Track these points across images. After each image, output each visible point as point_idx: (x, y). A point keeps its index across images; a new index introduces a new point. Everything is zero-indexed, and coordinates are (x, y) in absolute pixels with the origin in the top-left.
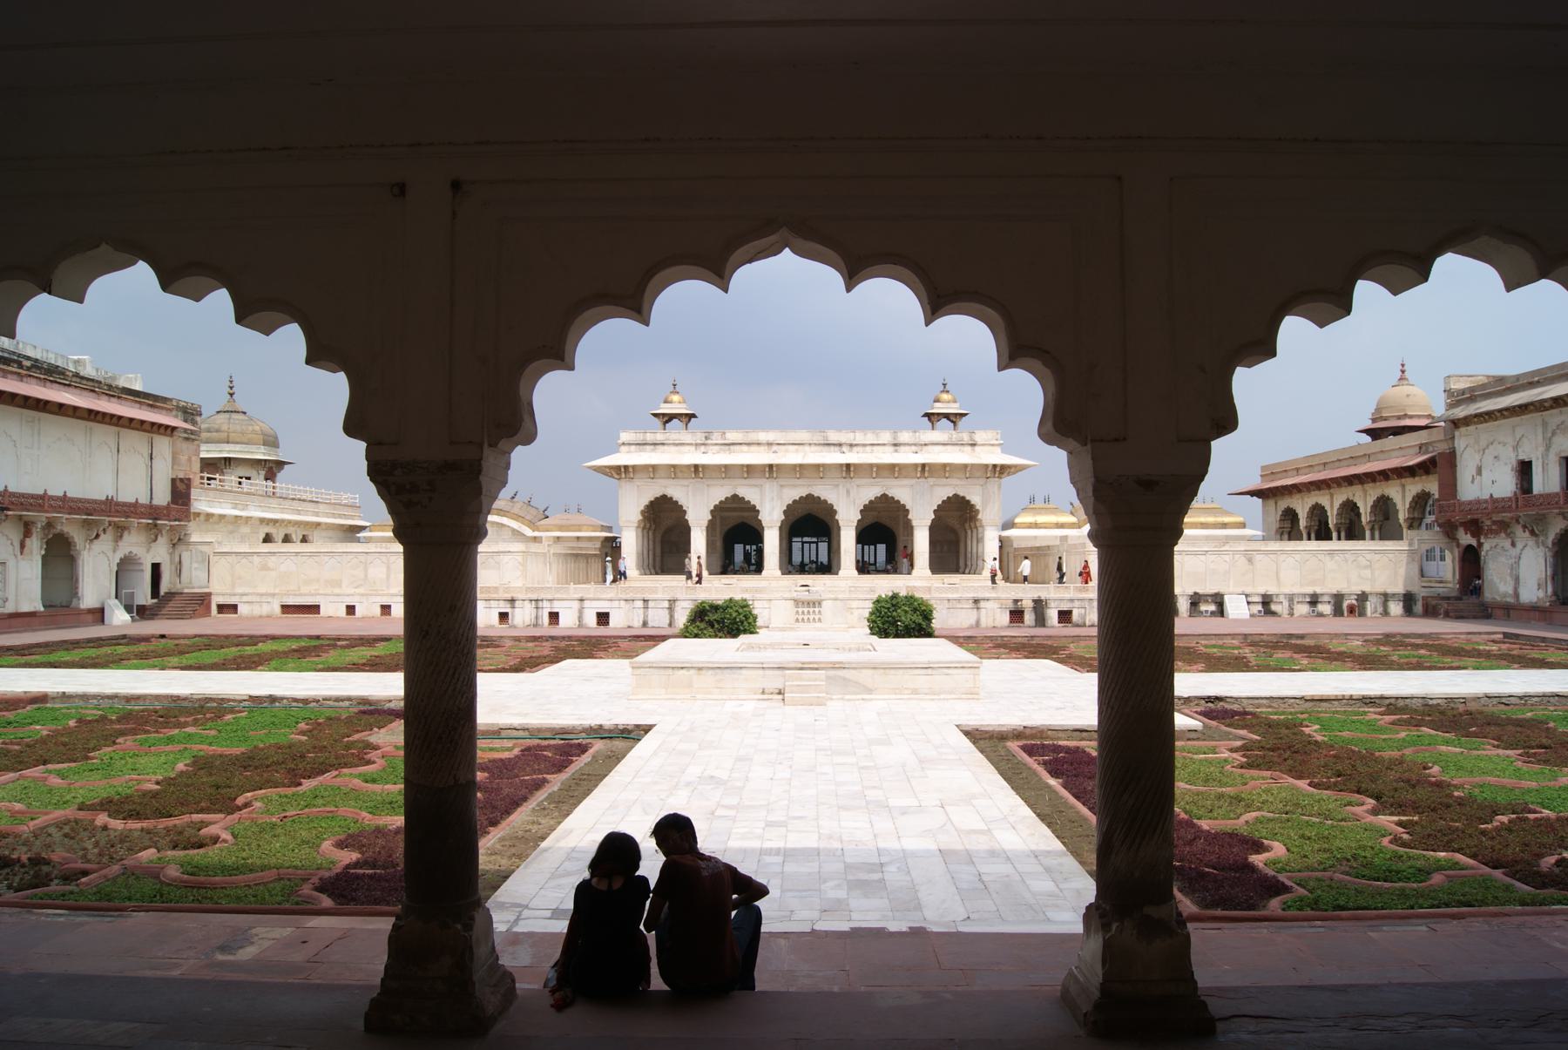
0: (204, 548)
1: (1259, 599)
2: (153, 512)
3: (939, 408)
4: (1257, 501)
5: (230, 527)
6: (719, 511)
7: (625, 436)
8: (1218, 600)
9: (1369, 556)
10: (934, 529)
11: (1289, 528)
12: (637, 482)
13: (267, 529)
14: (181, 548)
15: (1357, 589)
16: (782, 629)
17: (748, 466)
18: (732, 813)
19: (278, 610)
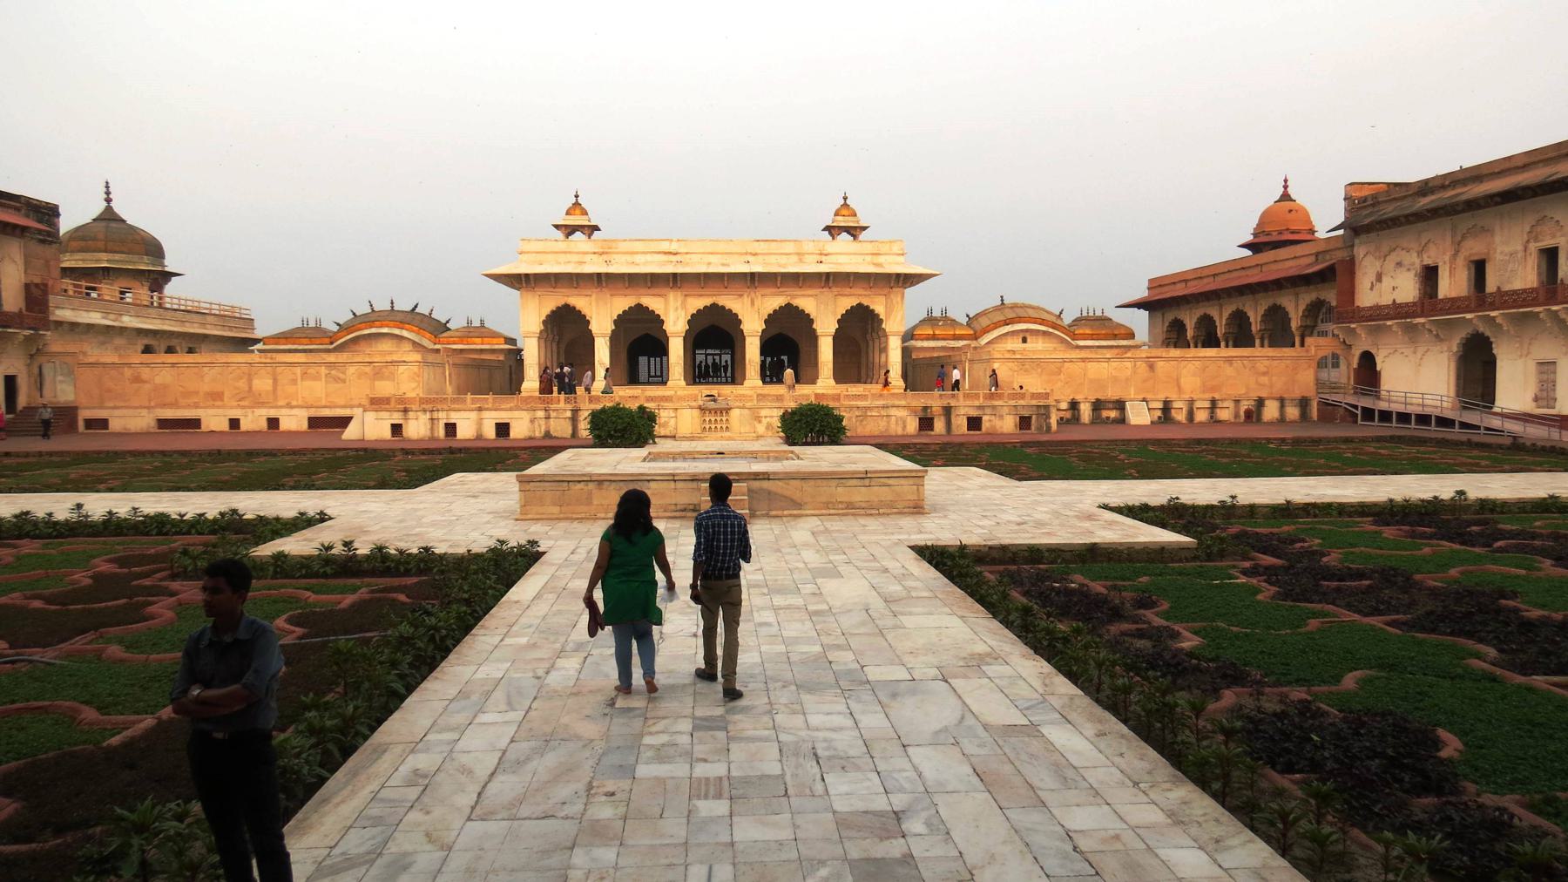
0: (68, 359)
1: (1160, 405)
3: (842, 221)
4: (1143, 315)
5: (101, 338)
6: (623, 322)
8: (1120, 405)
9: (1267, 363)
10: (837, 338)
11: (1175, 336)
12: (539, 291)
13: (146, 341)
14: (42, 359)
15: (1255, 395)
16: (692, 438)
19: (153, 423)
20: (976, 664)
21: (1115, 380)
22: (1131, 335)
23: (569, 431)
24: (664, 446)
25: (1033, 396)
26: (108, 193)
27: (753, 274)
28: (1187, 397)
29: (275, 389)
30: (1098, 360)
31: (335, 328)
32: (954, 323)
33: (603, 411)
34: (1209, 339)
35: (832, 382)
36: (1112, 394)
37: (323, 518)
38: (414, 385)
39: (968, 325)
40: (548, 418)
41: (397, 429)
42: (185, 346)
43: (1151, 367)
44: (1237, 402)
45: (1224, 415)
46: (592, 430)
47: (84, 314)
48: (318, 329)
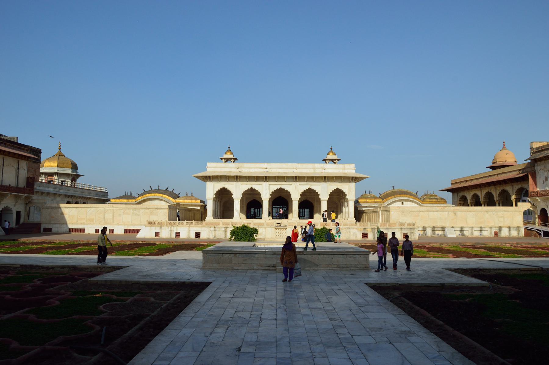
0: (39, 205)
2: (17, 189)
6: (245, 194)
7: (209, 165)
8: (443, 229)
10: (329, 202)
11: (463, 202)
15: (498, 225)
17: (257, 176)
18: (251, 350)
20: (404, 335)
25: (408, 225)
28: (470, 226)
29: (113, 218)
34: (477, 203)
36: (440, 224)
41: (157, 234)
43: (455, 214)
44: (491, 228)
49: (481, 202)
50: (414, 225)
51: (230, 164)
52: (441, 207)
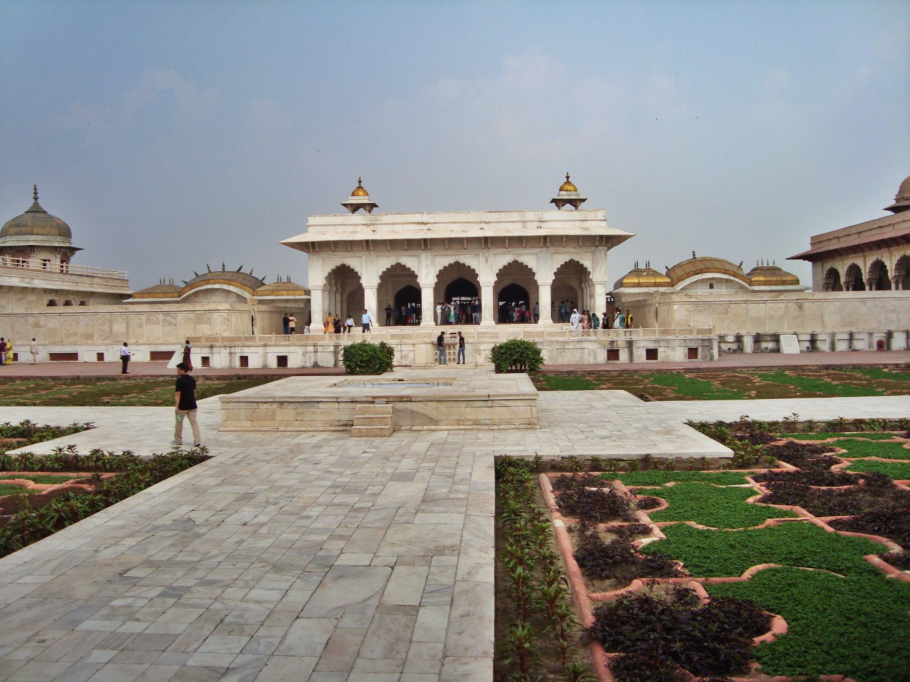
1: (808, 338)
3: (564, 195)
4: (808, 264)
5: (19, 296)
6: (387, 277)
7: (312, 220)
8: (776, 338)
11: (832, 282)
12: (323, 255)
13: (51, 297)
15: (885, 329)
16: (423, 367)
19: (48, 357)
21: (772, 317)
22: (797, 282)
23: (333, 362)
24: (398, 373)
25: (700, 332)
26: (36, 194)
27: (486, 239)
28: (830, 331)
29: (128, 332)
30: (757, 302)
31: (184, 285)
32: (655, 274)
33: (352, 347)
34: (858, 285)
35: (551, 321)
36: (769, 329)
37: (88, 427)
38: (225, 327)
39: (668, 275)
40: (316, 352)
42: (78, 300)
43: (800, 307)
44: (871, 334)
45: (858, 345)
46: (345, 361)
47: (7, 279)
48: (171, 286)
49: (864, 280)
50: (710, 331)
51: (360, 217)
52: (772, 294)
